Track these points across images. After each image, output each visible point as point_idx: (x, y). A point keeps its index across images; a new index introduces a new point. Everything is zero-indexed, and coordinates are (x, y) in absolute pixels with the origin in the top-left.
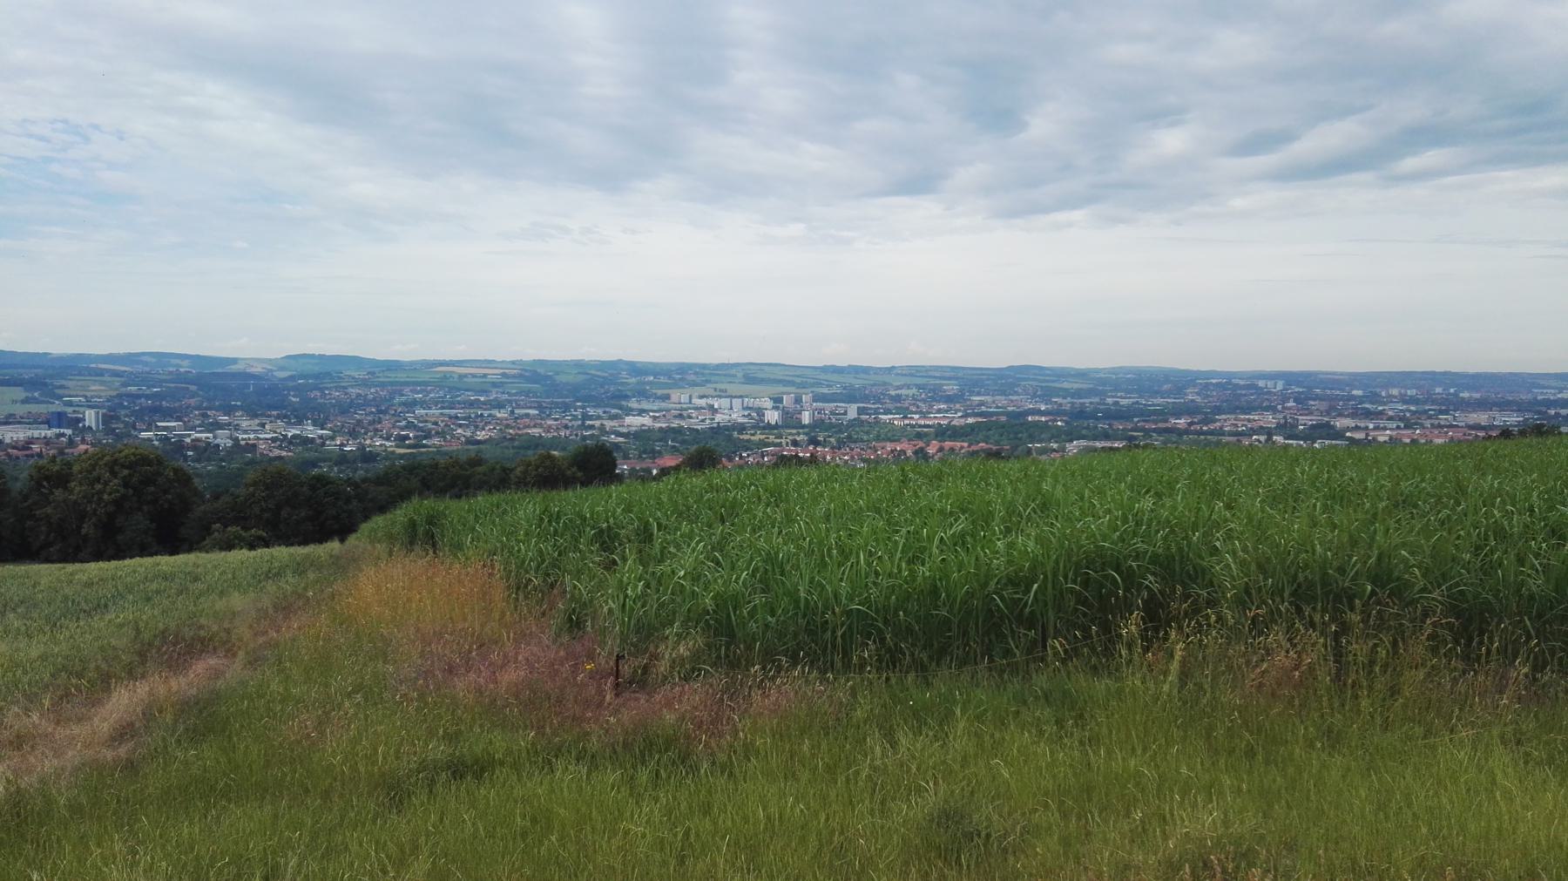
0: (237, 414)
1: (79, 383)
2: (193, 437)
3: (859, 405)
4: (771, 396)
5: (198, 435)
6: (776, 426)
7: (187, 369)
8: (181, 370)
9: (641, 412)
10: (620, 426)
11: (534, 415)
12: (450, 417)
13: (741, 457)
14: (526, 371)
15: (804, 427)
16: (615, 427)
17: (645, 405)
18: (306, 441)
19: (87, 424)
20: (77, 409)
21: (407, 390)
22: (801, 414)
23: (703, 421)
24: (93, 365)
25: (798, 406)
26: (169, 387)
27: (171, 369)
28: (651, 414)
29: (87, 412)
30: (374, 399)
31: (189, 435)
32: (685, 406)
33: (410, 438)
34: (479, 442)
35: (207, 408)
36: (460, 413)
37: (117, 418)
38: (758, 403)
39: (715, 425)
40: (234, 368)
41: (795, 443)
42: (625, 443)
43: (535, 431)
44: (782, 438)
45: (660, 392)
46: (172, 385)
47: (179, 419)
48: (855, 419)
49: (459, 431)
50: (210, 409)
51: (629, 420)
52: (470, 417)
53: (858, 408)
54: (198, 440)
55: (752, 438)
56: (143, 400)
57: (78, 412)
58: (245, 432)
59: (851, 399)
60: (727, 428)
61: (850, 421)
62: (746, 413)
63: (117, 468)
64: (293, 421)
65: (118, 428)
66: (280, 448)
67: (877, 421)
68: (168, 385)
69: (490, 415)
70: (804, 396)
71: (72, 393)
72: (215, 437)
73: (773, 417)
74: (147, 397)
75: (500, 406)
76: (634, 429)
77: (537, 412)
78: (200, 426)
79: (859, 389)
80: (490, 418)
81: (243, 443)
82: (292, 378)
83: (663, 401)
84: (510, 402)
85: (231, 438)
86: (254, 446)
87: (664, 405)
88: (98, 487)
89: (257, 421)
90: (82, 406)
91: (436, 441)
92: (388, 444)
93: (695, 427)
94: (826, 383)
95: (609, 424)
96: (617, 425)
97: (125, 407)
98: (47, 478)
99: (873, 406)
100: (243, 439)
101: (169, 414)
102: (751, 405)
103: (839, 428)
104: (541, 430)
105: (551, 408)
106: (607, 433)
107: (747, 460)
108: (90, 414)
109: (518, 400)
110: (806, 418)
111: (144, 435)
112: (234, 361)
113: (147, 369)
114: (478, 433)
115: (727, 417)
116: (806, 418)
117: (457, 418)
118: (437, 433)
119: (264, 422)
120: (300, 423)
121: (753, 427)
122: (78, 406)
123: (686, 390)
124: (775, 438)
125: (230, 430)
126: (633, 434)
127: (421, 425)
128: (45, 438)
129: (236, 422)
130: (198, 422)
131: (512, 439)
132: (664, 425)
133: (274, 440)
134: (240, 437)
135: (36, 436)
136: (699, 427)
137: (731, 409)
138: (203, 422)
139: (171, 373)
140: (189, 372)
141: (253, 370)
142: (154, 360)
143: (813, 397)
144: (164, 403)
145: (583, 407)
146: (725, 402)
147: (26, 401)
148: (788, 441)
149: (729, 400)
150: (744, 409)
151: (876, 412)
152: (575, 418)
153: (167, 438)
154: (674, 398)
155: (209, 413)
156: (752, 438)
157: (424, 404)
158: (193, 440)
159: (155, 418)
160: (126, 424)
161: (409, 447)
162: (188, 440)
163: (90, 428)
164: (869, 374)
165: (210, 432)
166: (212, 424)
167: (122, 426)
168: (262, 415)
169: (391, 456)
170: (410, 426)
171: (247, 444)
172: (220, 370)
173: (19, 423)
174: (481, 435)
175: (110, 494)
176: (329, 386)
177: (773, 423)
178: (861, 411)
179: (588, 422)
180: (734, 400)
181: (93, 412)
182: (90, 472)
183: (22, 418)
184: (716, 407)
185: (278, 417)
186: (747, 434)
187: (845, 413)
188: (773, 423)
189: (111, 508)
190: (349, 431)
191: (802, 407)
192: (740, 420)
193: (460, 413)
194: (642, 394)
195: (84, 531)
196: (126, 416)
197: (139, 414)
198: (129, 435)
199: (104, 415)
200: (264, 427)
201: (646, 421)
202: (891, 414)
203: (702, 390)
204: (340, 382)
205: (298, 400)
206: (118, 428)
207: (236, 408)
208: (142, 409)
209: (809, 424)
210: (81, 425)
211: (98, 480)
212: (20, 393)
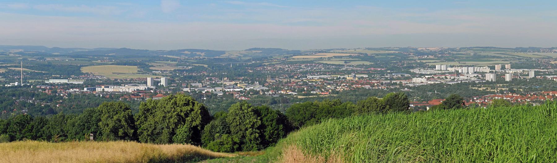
0: (225, 79)
1: (159, 64)
3: (535, 70)
4: (489, 65)
6: (492, 82)
7: (204, 57)
8: (201, 57)
9: (421, 75)
10: (409, 83)
11: (366, 78)
12: (324, 79)
13: (473, 100)
14: (362, 54)
15: (507, 82)
16: (407, 83)
17: (423, 71)
18: (257, 92)
19: (162, 84)
21: (303, 66)
22: (504, 75)
23: (454, 80)
24: (165, 56)
25: (504, 71)
26: (196, 66)
27: (197, 57)
28: (427, 77)
29: (162, 78)
30: (288, 70)
32: (443, 72)
33: (304, 90)
34: (338, 92)
35: (211, 76)
36: (329, 77)
38: (482, 70)
39: (460, 82)
40: (223, 56)
41: (502, 92)
42: (413, 92)
43: (367, 87)
44: (495, 89)
45: (430, 64)
46: (197, 65)
48: (533, 78)
49: (329, 86)
51: (415, 80)
52: (334, 79)
53: (535, 71)
55: (480, 89)
57: (158, 78)
59: (531, 67)
60: (465, 83)
61: (530, 79)
62: (476, 75)
64: (250, 82)
66: (244, 96)
67: (545, 79)
68: (195, 65)
69: (344, 78)
70: (506, 65)
71: (156, 69)
72: (215, 90)
73: (490, 77)
74: (187, 71)
75: (349, 73)
76: (418, 84)
77: (367, 76)
79: (535, 61)
80: (344, 80)
82: (249, 60)
83: (432, 69)
84: (353, 71)
87: (433, 71)
89: (233, 83)
90: (160, 75)
91: (318, 92)
92: (294, 93)
93: (449, 83)
94: (517, 57)
95: (404, 82)
96: (408, 82)
97: (177, 76)
99: (543, 71)
101: (195, 79)
102: (478, 71)
103: (525, 82)
104: (369, 86)
105: (374, 74)
106: (403, 87)
107: (476, 101)
108: (163, 79)
109: (358, 70)
110: (508, 78)
111: (185, 90)
112: (223, 52)
113: (187, 57)
114: (338, 87)
115: (466, 78)
116: (508, 78)
117: (327, 80)
118: (318, 88)
119: (237, 82)
120: (253, 83)
121: (479, 83)
122: (158, 75)
123: (444, 63)
124: (491, 89)
126: (417, 87)
127: (310, 83)
129: (224, 83)
131: (355, 91)
132: (432, 83)
133: (241, 92)
136: (451, 83)
137: (468, 73)
138: (210, 83)
139: (196, 59)
140: (204, 58)
141: (232, 57)
142: (189, 53)
143: (511, 65)
145: (391, 73)
146: (465, 69)
148: (498, 90)
149: (466, 68)
150: (475, 73)
151: (545, 73)
152: (387, 79)
154: (438, 67)
156: (480, 89)
157: (312, 73)
160: (178, 84)
161: (304, 95)
163: (163, 85)
164: (540, 52)
166: (214, 84)
168: (236, 80)
169: (296, 100)
170: (305, 84)
172: (217, 57)
174: (339, 89)
176: (266, 64)
177: (490, 80)
178: (536, 73)
179: (393, 82)
180: (469, 68)
184: (460, 72)
185: (243, 80)
186: (476, 87)
187: (528, 75)
188: (490, 80)
190: (276, 87)
191: (505, 71)
192: (473, 79)
193: (329, 77)
194: (422, 66)
200: (237, 85)
201: (424, 80)
202: (552, 75)
203: (452, 63)
204: (271, 62)
205: (252, 71)
207: (224, 76)
208: (185, 77)
209: (510, 81)
210: (159, 84)
212: (135, 69)
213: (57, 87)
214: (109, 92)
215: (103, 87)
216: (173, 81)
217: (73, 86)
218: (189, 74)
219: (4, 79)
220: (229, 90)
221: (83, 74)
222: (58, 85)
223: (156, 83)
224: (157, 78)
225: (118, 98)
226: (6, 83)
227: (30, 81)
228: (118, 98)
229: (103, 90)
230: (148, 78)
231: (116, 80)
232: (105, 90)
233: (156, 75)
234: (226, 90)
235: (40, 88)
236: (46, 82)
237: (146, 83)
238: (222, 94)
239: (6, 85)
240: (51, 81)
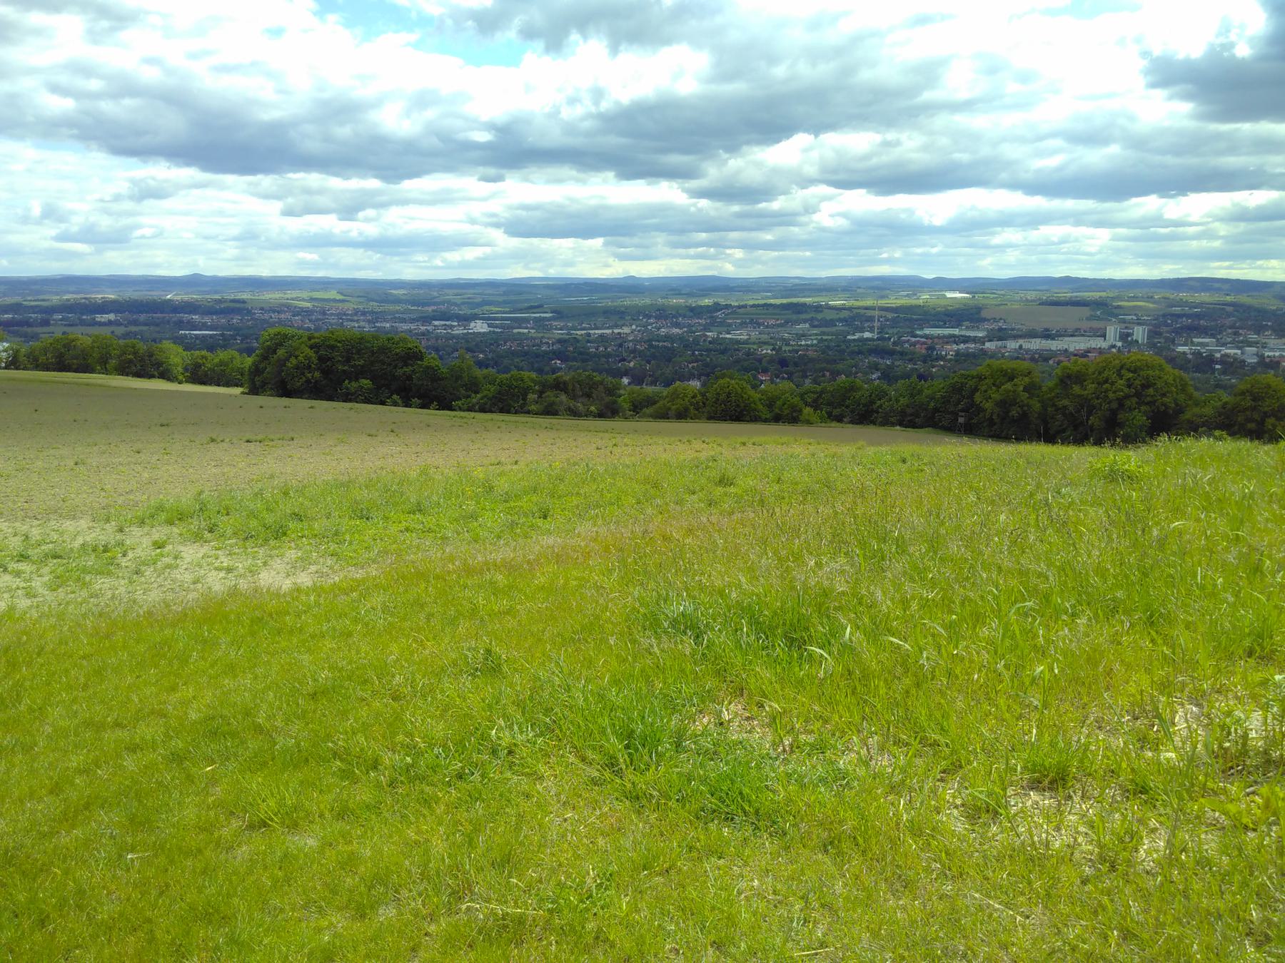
0: (1266, 333)
2: (1222, 352)
5: (1228, 351)
20: (1128, 325)
26: (1209, 308)
31: (1220, 351)
37: (1159, 334)
47: (1213, 336)
50: (1242, 328)
54: (1227, 355)
56: (1184, 319)
58: (1272, 350)
63: (1123, 372)
65: (1160, 342)
72: (1242, 353)
78: (1229, 343)
81: (1267, 360)
85: (1257, 355)
86: (1278, 363)
88: (1106, 386)
90: (1133, 323)
98: (1069, 376)
100: (1268, 357)
101: (1204, 332)
111: (1180, 349)
122: (1129, 323)
125: (1258, 347)
128: (1100, 348)
130: (1229, 340)
134: (1266, 354)
135: (1093, 346)
144: (1201, 322)
147: (1089, 319)
153: (1200, 353)
155: (1240, 331)
158: (1222, 356)
159: (1192, 335)
160: (1167, 339)
162: (1218, 355)
165: (1238, 348)
166: (1242, 342)
167: (1162, 340)
171: (1271, 361)
173: (1083, 335)
175: (1115, 392)
181: (1141, 328)
182: (1100, 373)
183: (1085, 332)
189: (1114, 405)
195: (1090, 422)
196: (1167, 332)
197: (1178, 332)
198: (1169, 349)
199: (1149, 331)
206: (1160, 342)
207: (1265, 328)
210: (1129, 339)
211: (1106, 381)
212: (1086, 311)
213: (936, 340)
214: (1031, 351)
215: (1021, 341)
216: (1159, 334)
217: (966, 340)
218: (1193, 321)
219: (847, 328)
220: (1271, 354)
221: (985, 320)
222: (939, 337)
223: (1124, 337)
224: (1126, 328)
225: (1046, 360)
226: (849, 334)
227: (890, 331)
228: (1046, 360)
229: (1021, 347)
230: (1108, 328)
231: (1047, 330)
232: (1024, 347)
233: (1125, 322)
234: (1266, 354)
235: (908, 341)
236: (918, 332)
237: (1104, 336)
238: (1255, 361)
239: (849, 337)
240: (927, 331)
